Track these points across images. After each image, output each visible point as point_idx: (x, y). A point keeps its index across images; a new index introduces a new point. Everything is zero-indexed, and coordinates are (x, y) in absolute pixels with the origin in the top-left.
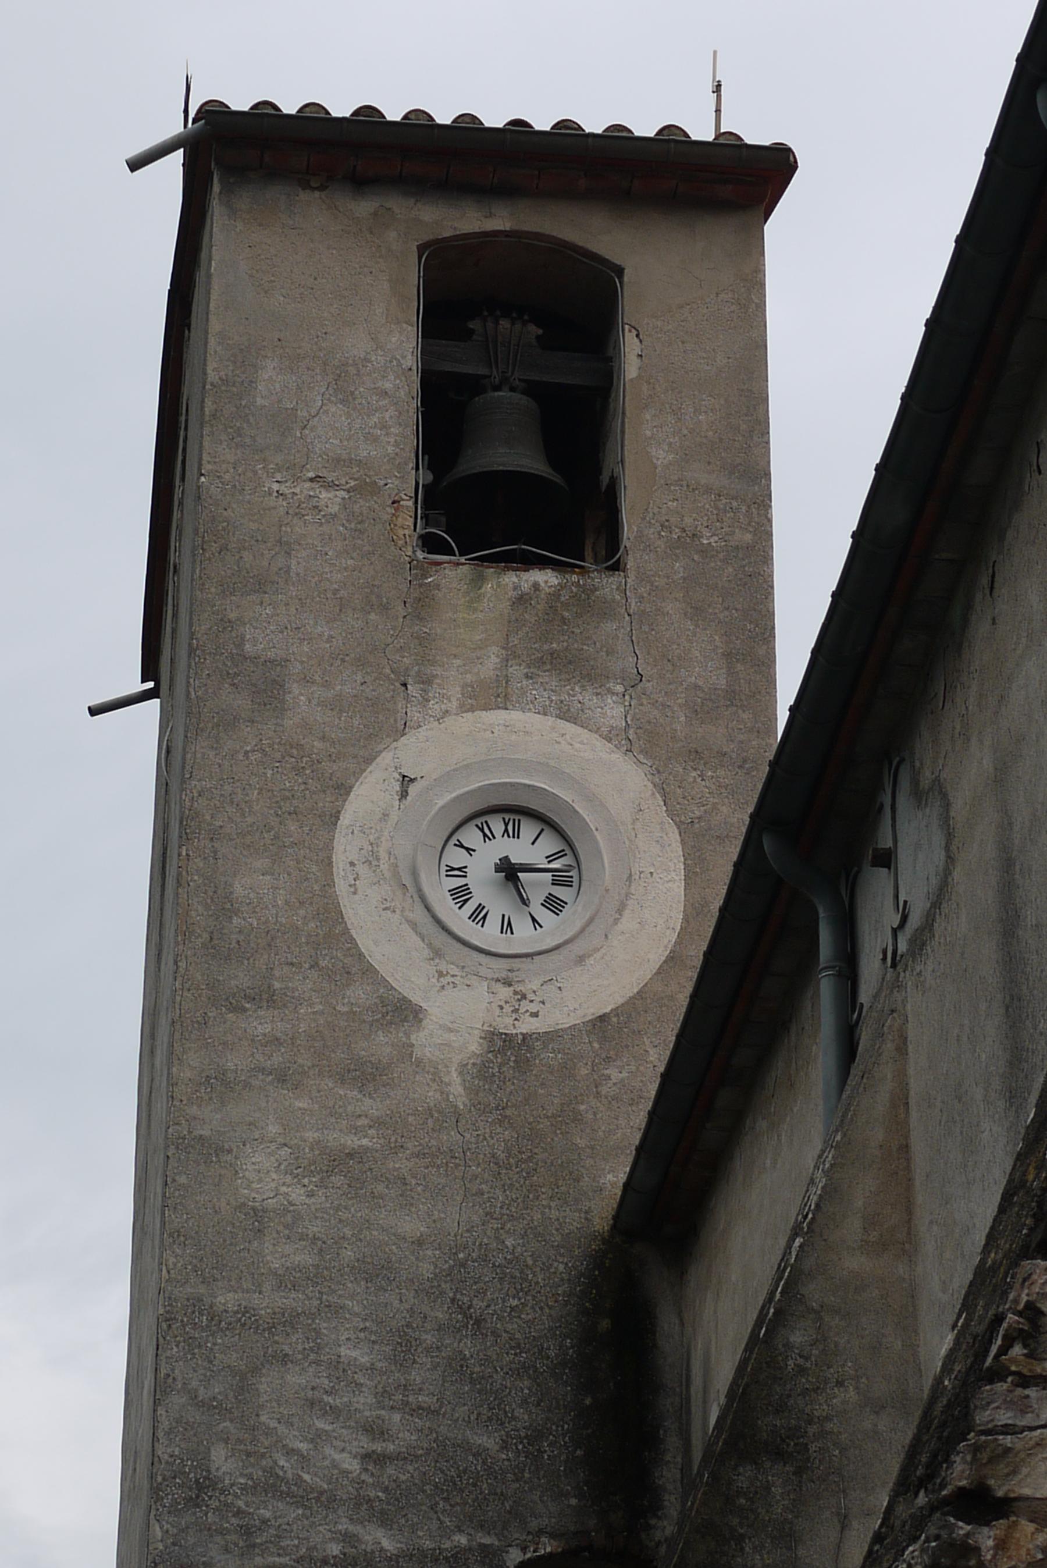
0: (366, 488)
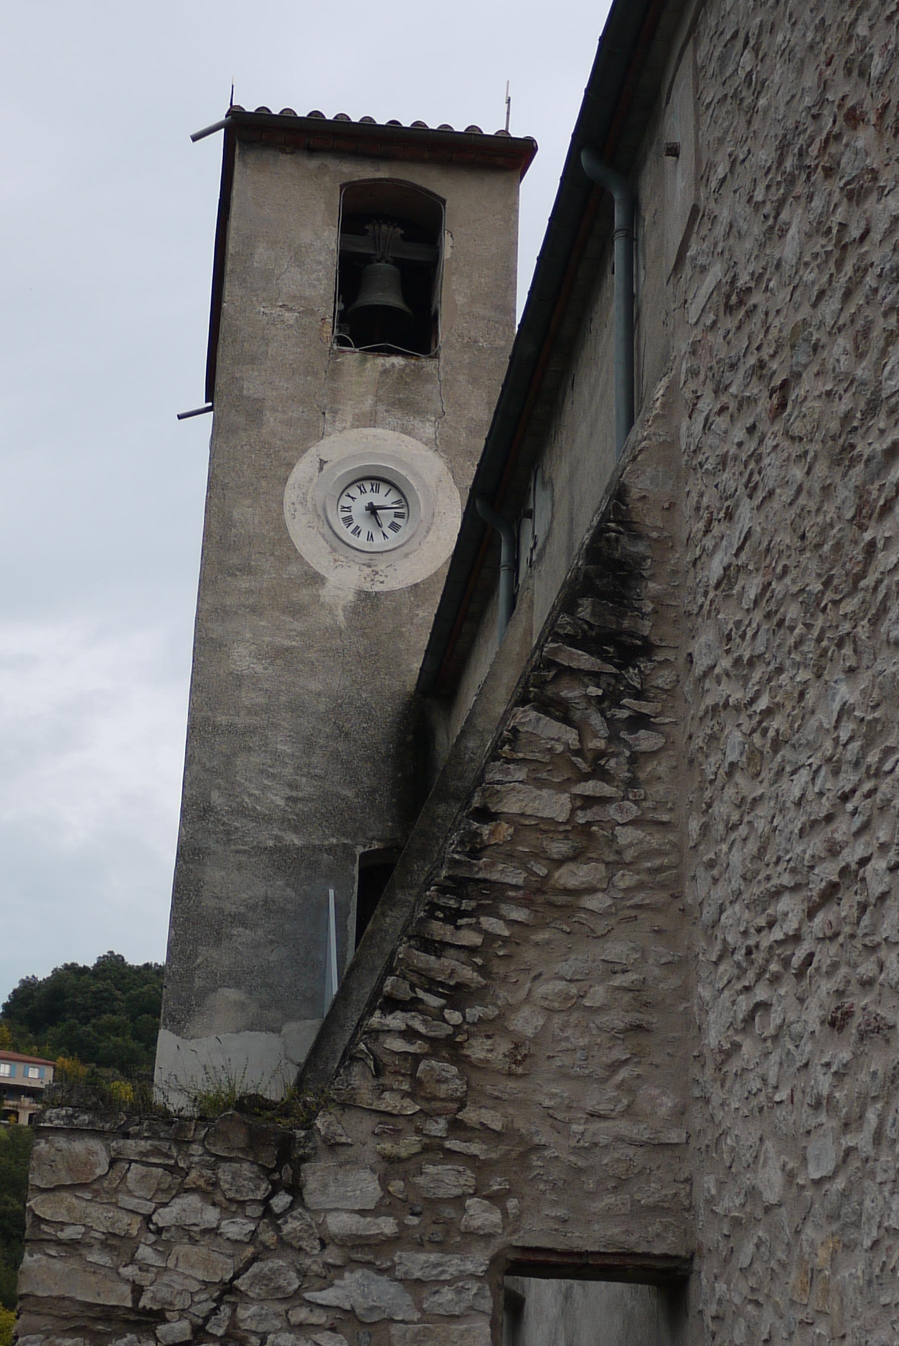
0: (308, 312)
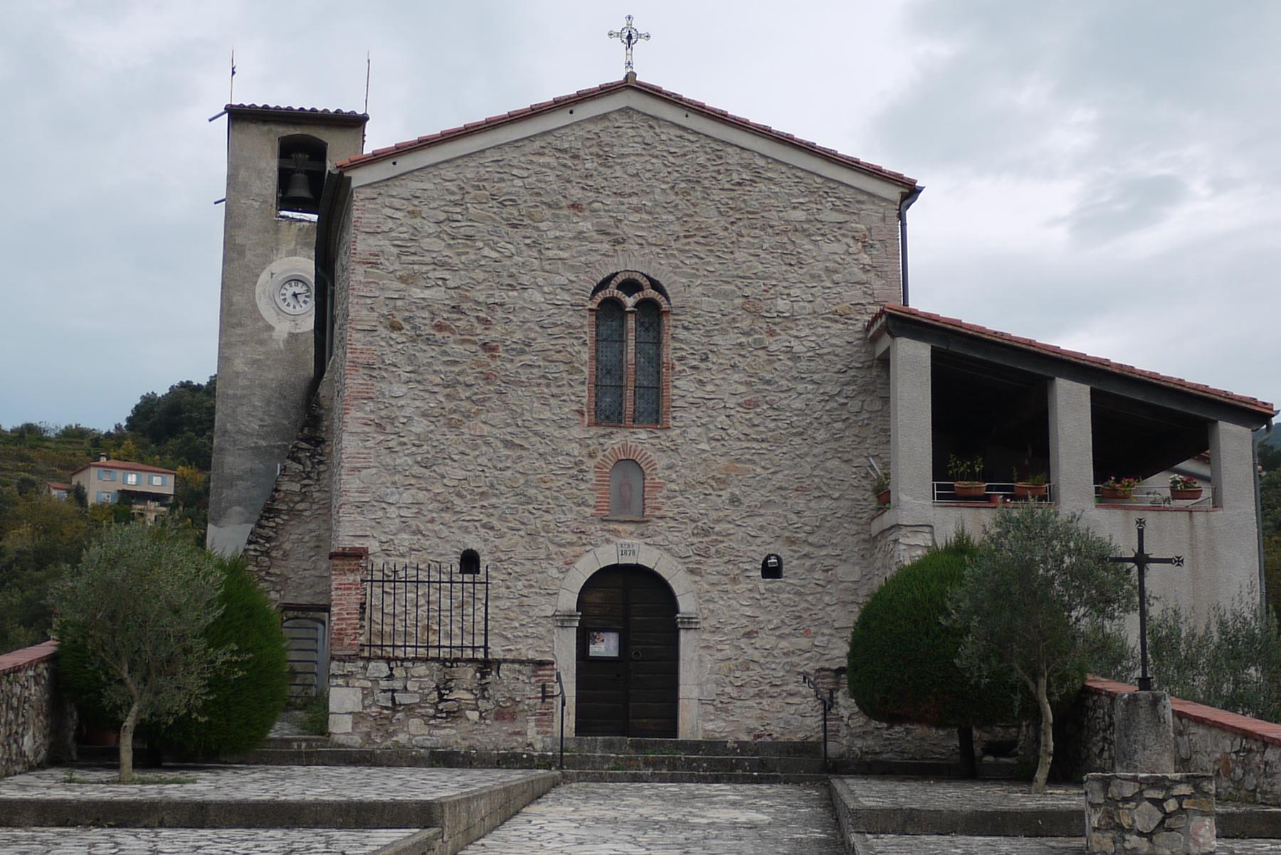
0: (265, 202)
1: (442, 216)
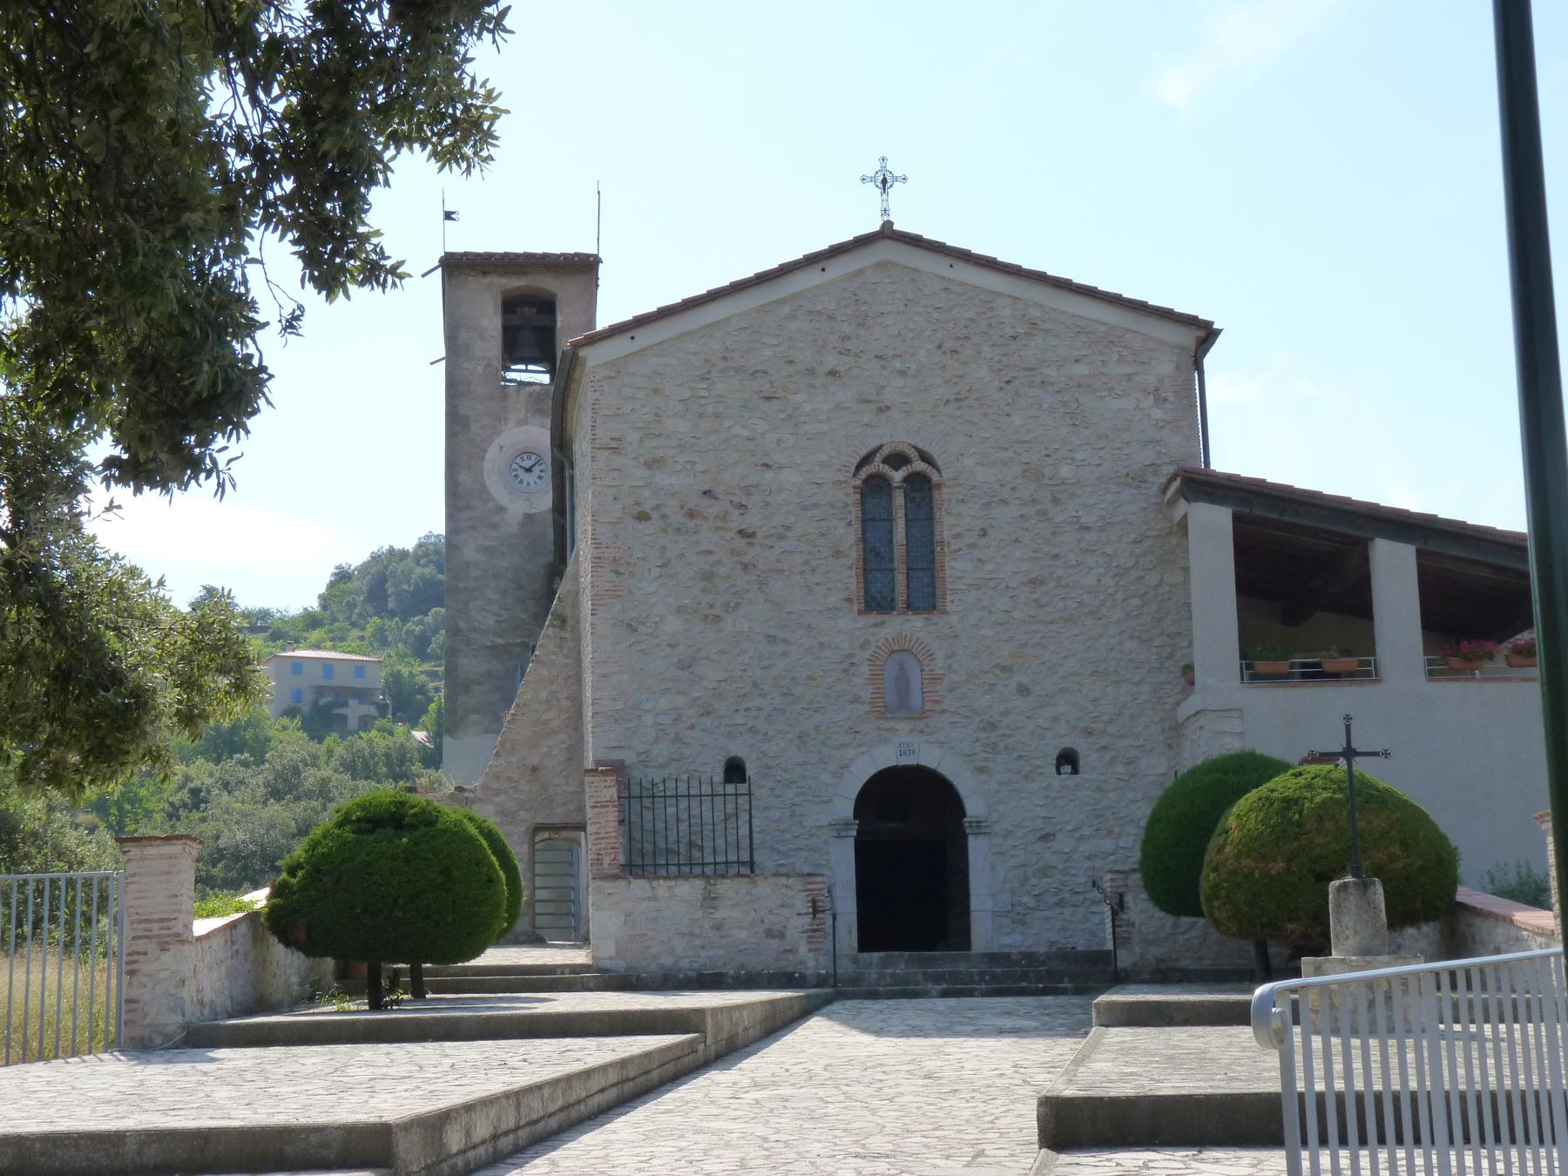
0: (489, 365)
1: (687, 393)
